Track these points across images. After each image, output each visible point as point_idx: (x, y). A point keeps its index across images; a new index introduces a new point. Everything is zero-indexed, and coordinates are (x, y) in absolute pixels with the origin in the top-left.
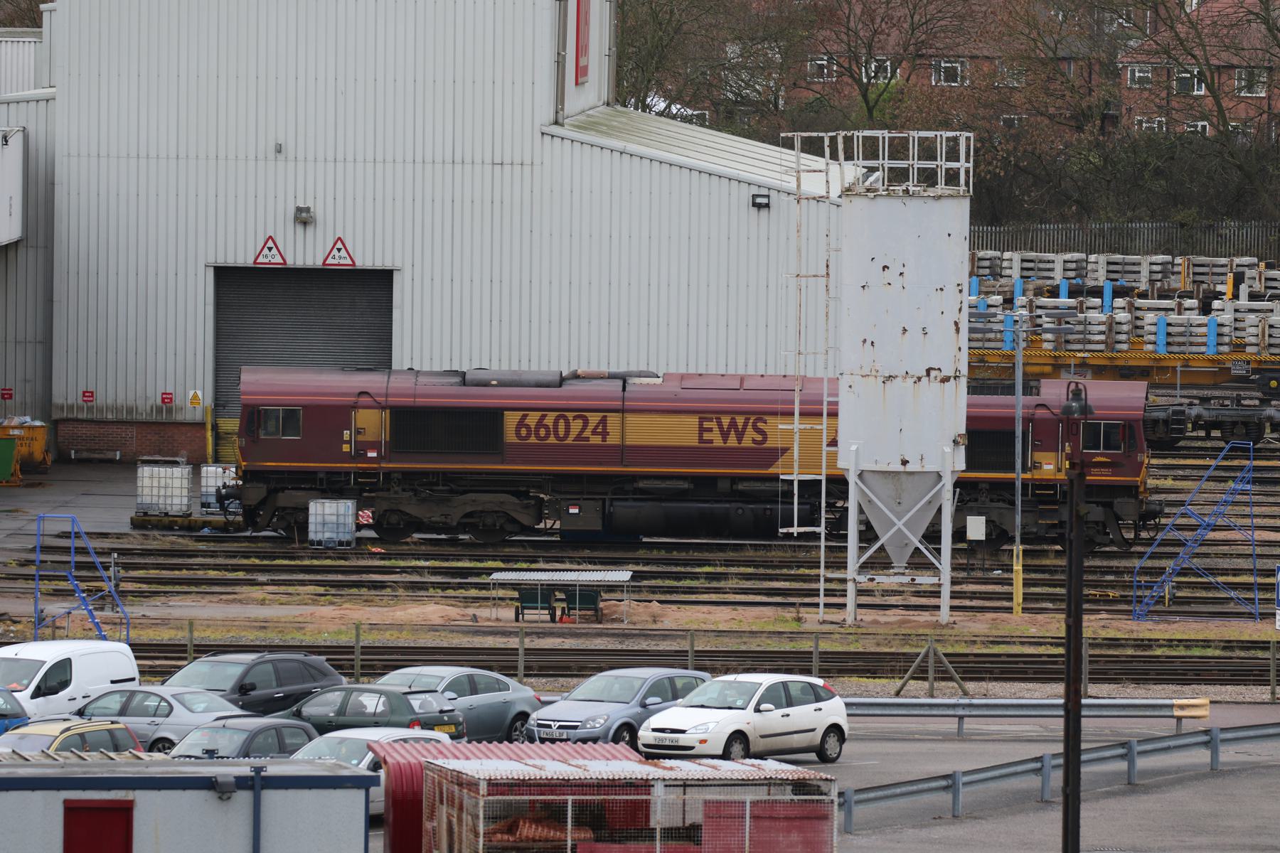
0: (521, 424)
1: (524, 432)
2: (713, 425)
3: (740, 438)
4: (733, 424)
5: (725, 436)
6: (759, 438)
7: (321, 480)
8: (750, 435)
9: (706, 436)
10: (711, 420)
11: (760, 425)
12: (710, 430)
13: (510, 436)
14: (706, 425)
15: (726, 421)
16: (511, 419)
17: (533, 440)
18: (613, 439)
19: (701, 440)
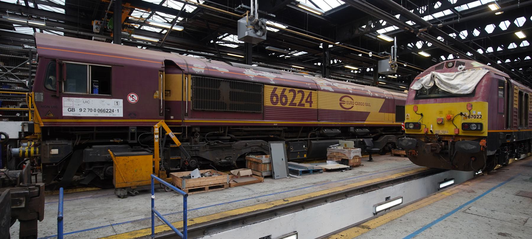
0: (273, 94)
1: (275, 99)
7: (133, 134)
13: (268, 102)
16: (268, 91)
17: (279, 105)
18: (314, 106)
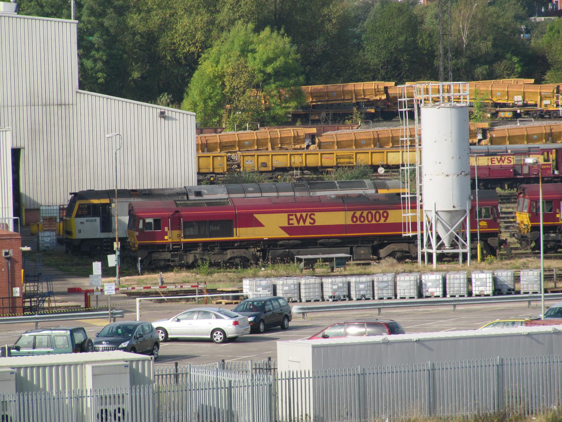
2: (294, 217)
3: (304, 221)
4: (301, 216)
5: (298, 222)
6: (312, 221)
8: (308, 220)
9: (291, 222)
10: (292, 215)
11: (312, 216)
12: (292, 219)
14: (291, 217)
15: (298, 215)
19: (289, 224)
